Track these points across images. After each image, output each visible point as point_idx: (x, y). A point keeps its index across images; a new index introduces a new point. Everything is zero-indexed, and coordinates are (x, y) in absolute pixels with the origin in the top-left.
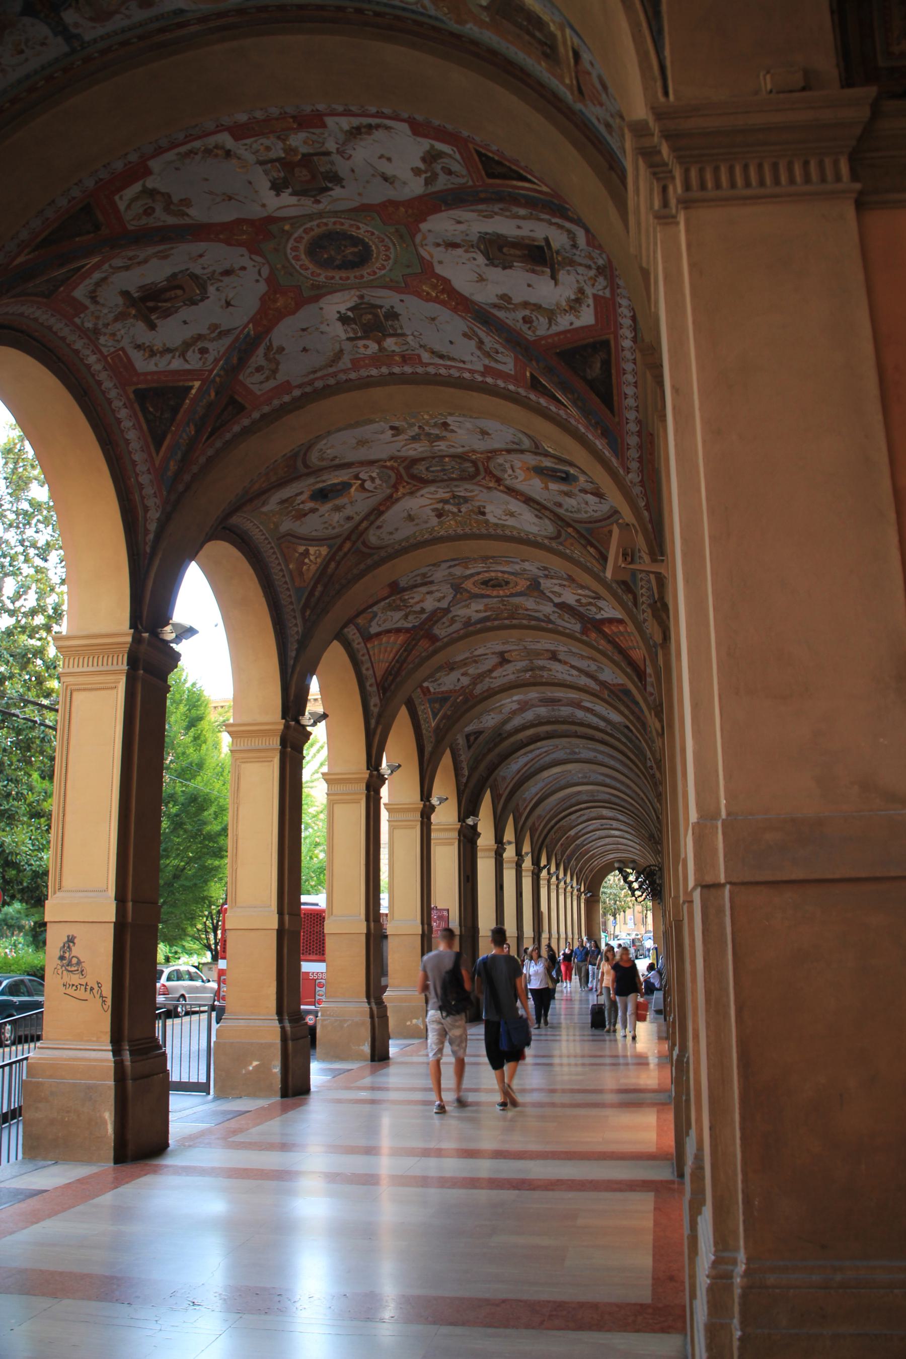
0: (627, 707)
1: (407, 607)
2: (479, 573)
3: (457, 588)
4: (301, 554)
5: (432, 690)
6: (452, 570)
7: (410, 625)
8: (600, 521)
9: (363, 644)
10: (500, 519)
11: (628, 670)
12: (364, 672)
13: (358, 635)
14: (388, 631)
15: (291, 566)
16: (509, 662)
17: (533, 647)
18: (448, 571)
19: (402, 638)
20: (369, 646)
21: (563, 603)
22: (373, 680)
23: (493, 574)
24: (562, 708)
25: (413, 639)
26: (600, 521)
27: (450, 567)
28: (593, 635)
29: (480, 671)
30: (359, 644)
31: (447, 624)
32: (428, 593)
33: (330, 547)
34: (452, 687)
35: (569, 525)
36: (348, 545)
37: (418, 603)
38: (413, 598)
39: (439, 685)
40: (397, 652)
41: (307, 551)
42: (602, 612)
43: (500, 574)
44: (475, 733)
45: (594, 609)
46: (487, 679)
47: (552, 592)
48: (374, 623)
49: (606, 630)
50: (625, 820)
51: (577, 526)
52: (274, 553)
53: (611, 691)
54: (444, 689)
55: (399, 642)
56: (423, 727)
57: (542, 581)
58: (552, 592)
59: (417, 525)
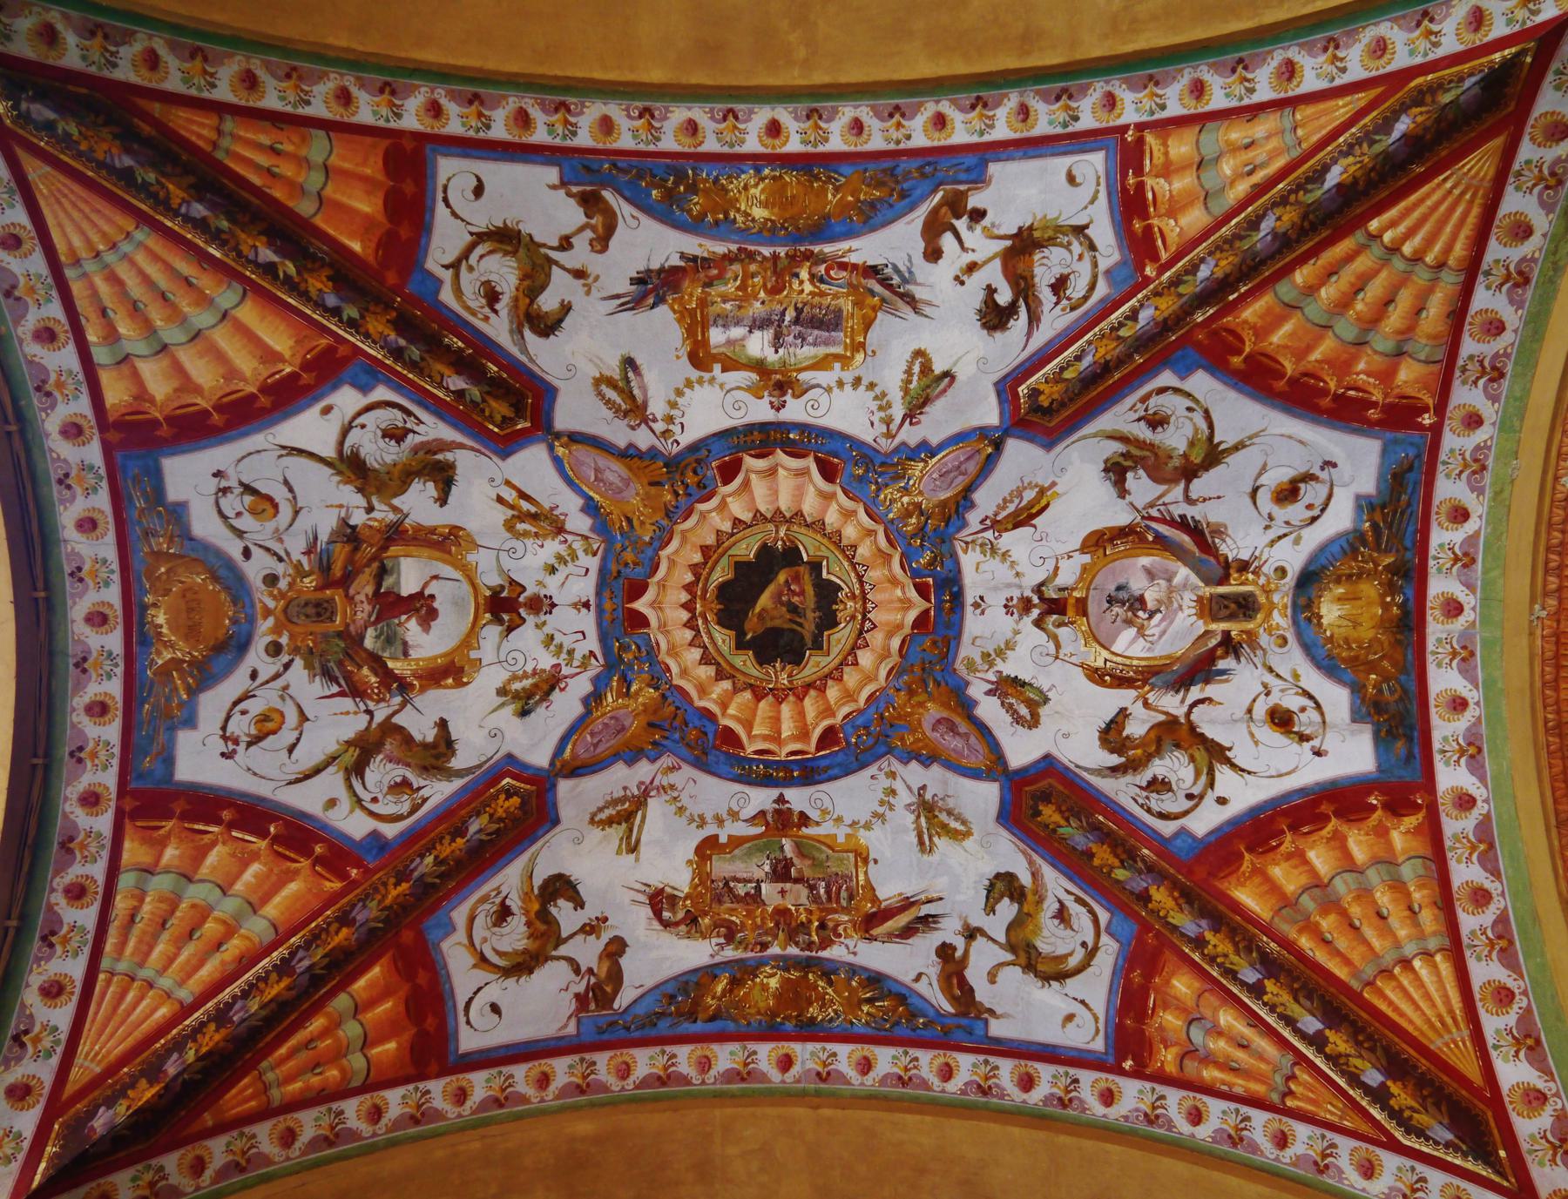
7: (356, 826)
9: (104, 823)
14: (250, 815)
20: (133, 851)
21: (1048, 766)
25: (344, 919)
30: (91, 800)
40: (246, 962)
47: (1008, 687)
49: (1247, 896)
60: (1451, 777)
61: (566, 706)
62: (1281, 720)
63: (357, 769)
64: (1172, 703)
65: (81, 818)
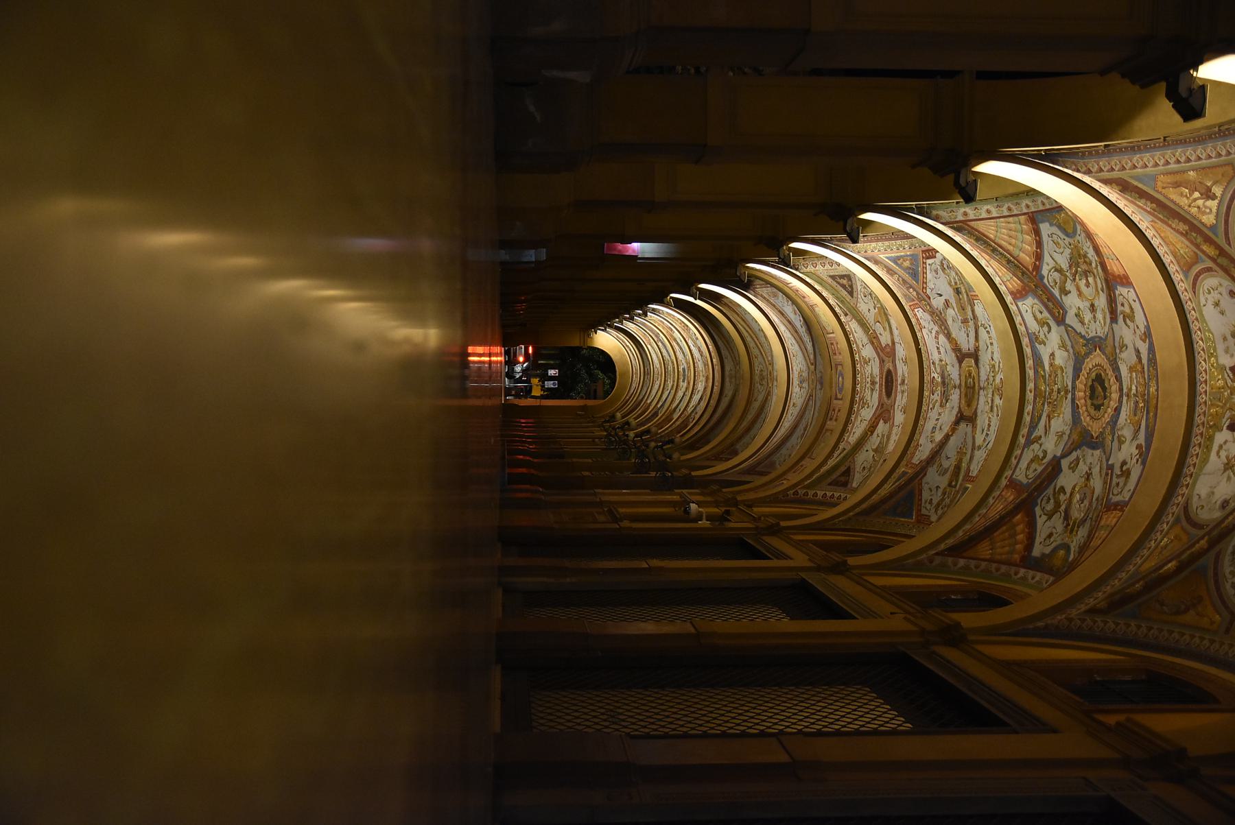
0: (891, 495)
1: (1074, 275)
2: (1119, 378)
3: (1095, 344)
4: (1209, 189)
5: (929, 261)
6: (1131, 350)
7: (1045, 272)
8: (1218, 589)
9: (1025, 211)
10: (1221, 447)
11: (960, 533)
12: (986, 207)
13: (1041, 208)
14: (1039, 244)
15: (1191, 173)
16: (960, 361)
17: (982, 400)
18: (1131, 346)
19: (1027, 260)
20: (1022, 218)
22: (972, 217)
23: (1115, 396)
24: (876, 395)
25: (1023, 273)
26: (1218, 589)
27: (1138, 351)
28: (1010, 496)
29: (950, 322)
31: (1039, 316)
32: (1092, 305)
33: (1213, 228)
34: (931, 285)
35: (1213, 544)
36: (1211, 251)
37: (1078, 289)
38: (1088, 285)
39: (936, 271)
40: (1008, 251)
41: (1213, 197)
42: (1044, 518)
43: (1113, 404)
44: (851, 286)
45: (1050, 507)
46: (936, 328)
47: (1078, 459)
48: (1055, 230)
49: (1019, 517)
50: (693, 403)
51: (1213, 553)
52: (1219, 155)
53: (911, 480)
54: (929, 276)
55: (1022, 255)
56: (880, 244)
57: (1097, 453)
58: (1078, 459)
59: (1225, 339)
60: (1022, 571)
61: (1079, 327)
62: (1050, 535)
63: (1056, 270)
64: (1063, 507)
65: (1023, 205)
